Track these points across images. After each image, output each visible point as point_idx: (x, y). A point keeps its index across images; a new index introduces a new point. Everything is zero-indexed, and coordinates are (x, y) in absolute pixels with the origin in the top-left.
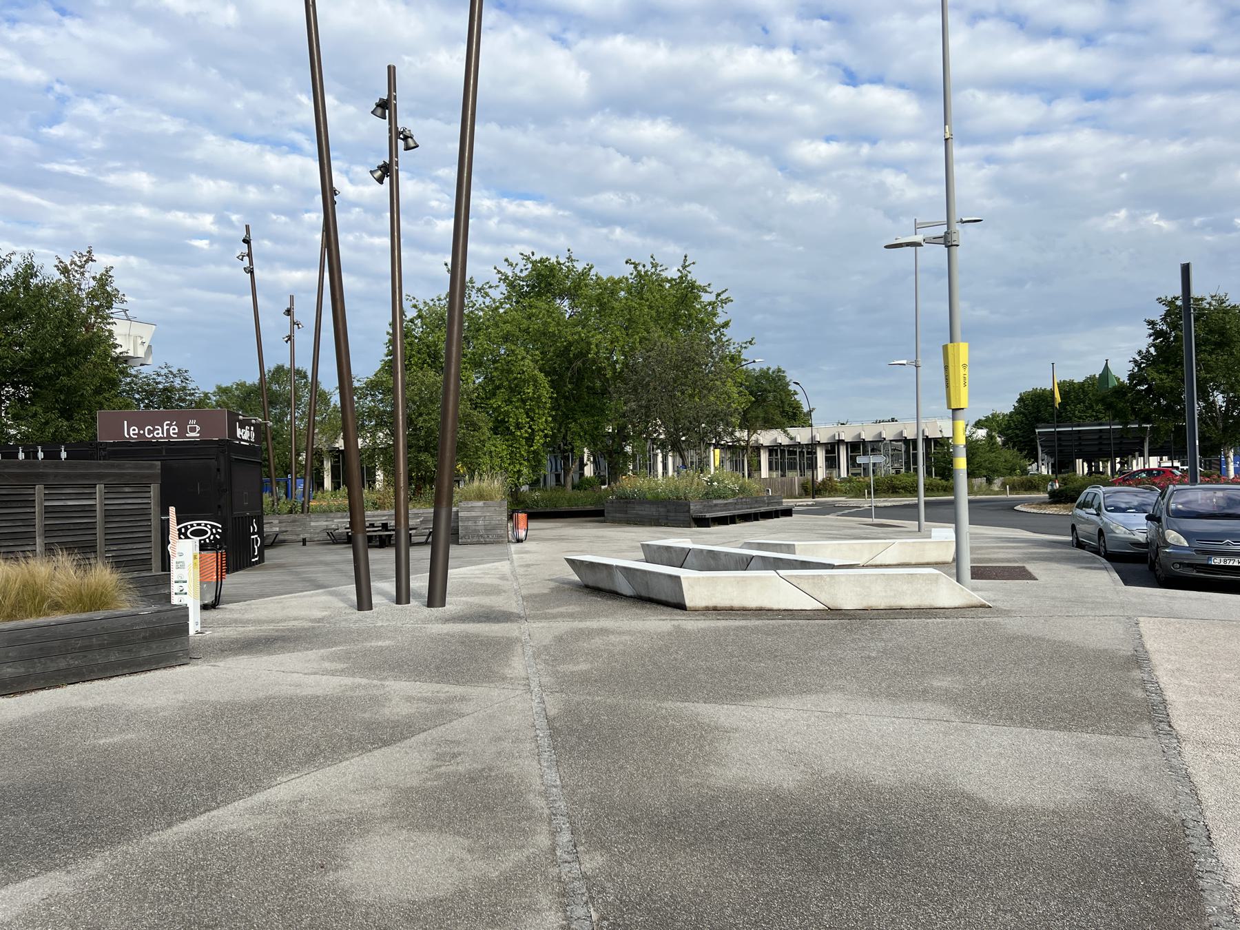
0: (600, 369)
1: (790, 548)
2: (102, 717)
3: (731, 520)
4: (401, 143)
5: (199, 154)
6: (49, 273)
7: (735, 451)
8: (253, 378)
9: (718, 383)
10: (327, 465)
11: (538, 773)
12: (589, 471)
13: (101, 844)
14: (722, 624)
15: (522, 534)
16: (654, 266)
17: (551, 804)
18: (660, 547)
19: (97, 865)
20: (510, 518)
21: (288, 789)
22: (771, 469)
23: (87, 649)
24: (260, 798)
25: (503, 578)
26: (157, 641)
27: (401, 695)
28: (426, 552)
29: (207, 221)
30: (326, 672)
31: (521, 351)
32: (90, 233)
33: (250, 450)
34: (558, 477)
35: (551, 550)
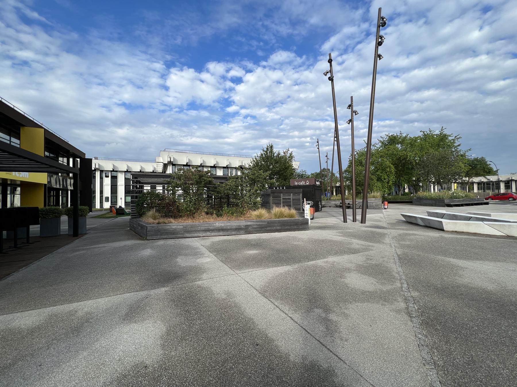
0: (411, 162)
1: (489, 215)
2: (294, 238)
3: (462, 205)
4: (354, 114)
5: (307, 126)
6: (282, 154)
7: (463, 185)
8: (318, 171)
9: (456, 163)
10: (334, 190)
11: (396, 268)
12: (407, 191)
13: (297, 262)
14: (459, 236)
15: (386, 207)
16: (430, 131)
17: (400, 276)
18: (433, 213)
19: (296, 266)
20: (383, 203)
21: (331, 259)
22: (478, 189)
23: (291, 225)
24: (326, 260)
25: (381, 218)
26: (303, 225)
27: (356, 243)
28: (360, 210)
29: (308, 139)
30: (337, 236)
31: (385, 160)
32: (287, 145)
33: (319, 186)
34: (396, 192)
35: (396, 212)
